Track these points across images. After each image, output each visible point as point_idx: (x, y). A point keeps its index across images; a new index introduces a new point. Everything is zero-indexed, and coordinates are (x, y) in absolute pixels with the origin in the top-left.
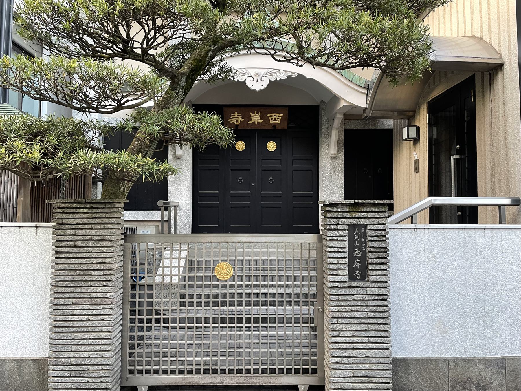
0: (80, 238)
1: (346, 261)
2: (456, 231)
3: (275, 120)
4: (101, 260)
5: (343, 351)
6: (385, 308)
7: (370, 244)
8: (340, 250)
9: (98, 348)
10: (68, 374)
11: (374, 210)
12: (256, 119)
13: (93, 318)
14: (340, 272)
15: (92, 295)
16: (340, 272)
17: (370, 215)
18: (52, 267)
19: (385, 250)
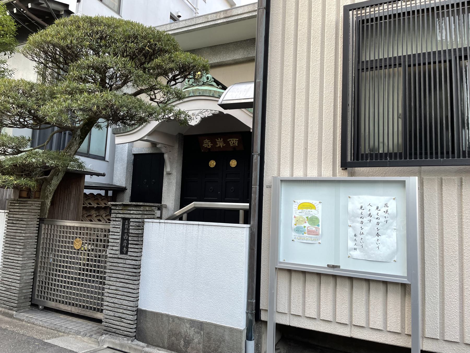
0: (14, 219)
1: (119, 241)
2: (182, 225)
3: (234, 144)
4: (20, 231)
5: (111, 298)
6: (138, 275)
7: (131, 231)
8: (116, 234)
9: (15, 277)
10: (4, 289)
11: (134, 209)
12: (220, 143)
13: (15, 261)
14: (114, 248)
15: (16, 249)
16: (114, 248)
17: (132, 212)
18: (5, 233)
19: (141, 236)
